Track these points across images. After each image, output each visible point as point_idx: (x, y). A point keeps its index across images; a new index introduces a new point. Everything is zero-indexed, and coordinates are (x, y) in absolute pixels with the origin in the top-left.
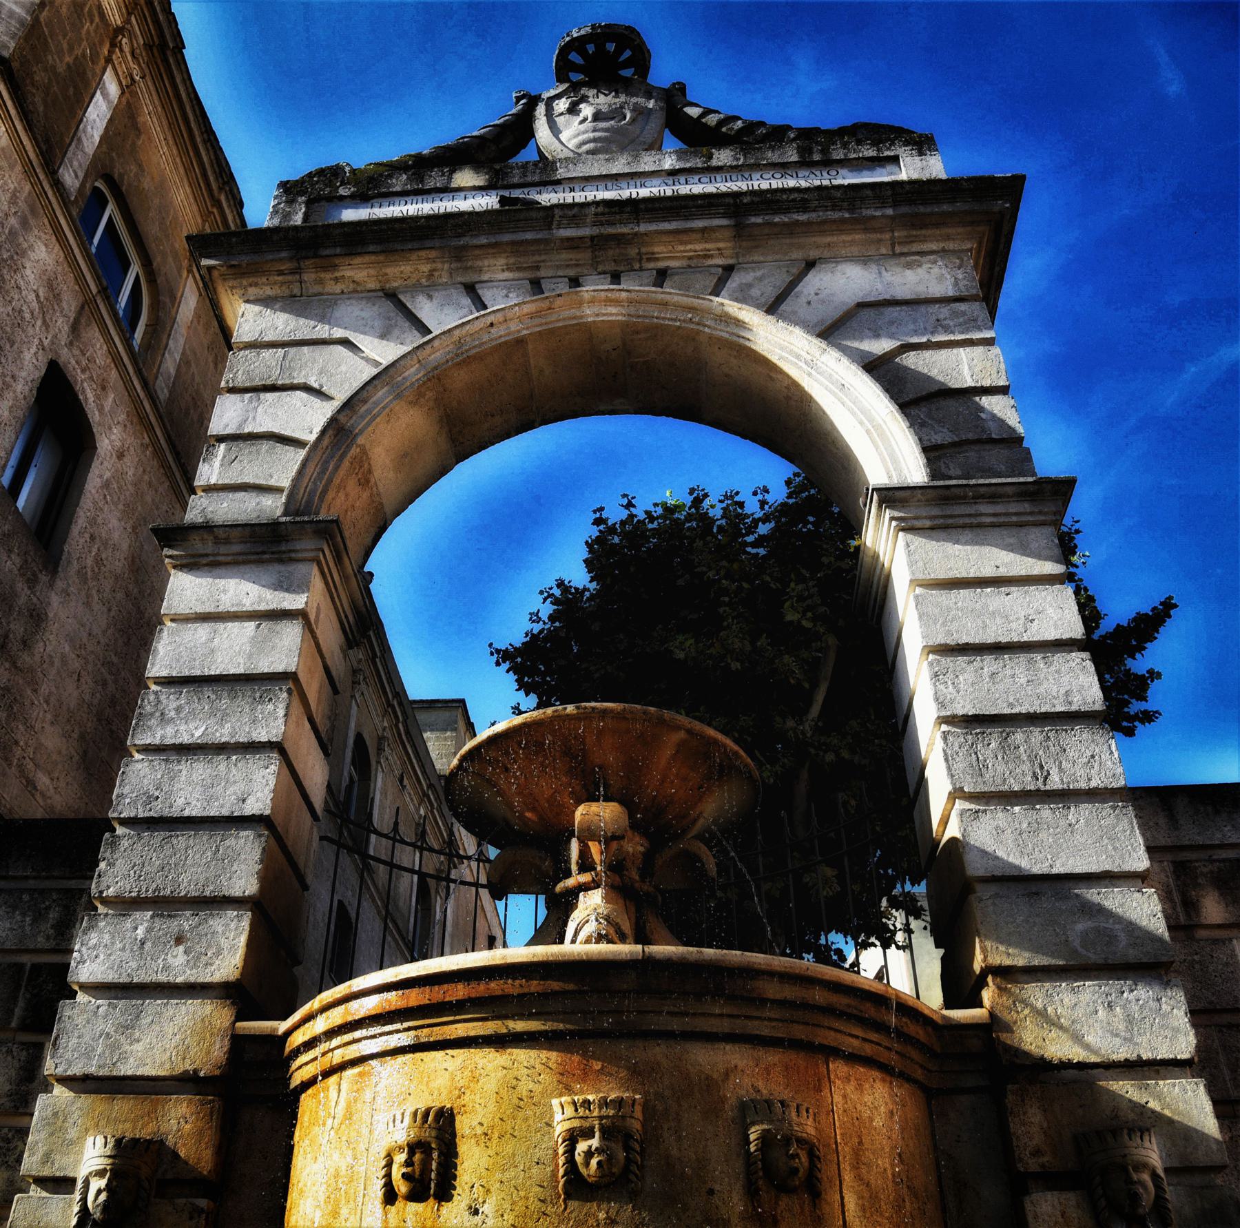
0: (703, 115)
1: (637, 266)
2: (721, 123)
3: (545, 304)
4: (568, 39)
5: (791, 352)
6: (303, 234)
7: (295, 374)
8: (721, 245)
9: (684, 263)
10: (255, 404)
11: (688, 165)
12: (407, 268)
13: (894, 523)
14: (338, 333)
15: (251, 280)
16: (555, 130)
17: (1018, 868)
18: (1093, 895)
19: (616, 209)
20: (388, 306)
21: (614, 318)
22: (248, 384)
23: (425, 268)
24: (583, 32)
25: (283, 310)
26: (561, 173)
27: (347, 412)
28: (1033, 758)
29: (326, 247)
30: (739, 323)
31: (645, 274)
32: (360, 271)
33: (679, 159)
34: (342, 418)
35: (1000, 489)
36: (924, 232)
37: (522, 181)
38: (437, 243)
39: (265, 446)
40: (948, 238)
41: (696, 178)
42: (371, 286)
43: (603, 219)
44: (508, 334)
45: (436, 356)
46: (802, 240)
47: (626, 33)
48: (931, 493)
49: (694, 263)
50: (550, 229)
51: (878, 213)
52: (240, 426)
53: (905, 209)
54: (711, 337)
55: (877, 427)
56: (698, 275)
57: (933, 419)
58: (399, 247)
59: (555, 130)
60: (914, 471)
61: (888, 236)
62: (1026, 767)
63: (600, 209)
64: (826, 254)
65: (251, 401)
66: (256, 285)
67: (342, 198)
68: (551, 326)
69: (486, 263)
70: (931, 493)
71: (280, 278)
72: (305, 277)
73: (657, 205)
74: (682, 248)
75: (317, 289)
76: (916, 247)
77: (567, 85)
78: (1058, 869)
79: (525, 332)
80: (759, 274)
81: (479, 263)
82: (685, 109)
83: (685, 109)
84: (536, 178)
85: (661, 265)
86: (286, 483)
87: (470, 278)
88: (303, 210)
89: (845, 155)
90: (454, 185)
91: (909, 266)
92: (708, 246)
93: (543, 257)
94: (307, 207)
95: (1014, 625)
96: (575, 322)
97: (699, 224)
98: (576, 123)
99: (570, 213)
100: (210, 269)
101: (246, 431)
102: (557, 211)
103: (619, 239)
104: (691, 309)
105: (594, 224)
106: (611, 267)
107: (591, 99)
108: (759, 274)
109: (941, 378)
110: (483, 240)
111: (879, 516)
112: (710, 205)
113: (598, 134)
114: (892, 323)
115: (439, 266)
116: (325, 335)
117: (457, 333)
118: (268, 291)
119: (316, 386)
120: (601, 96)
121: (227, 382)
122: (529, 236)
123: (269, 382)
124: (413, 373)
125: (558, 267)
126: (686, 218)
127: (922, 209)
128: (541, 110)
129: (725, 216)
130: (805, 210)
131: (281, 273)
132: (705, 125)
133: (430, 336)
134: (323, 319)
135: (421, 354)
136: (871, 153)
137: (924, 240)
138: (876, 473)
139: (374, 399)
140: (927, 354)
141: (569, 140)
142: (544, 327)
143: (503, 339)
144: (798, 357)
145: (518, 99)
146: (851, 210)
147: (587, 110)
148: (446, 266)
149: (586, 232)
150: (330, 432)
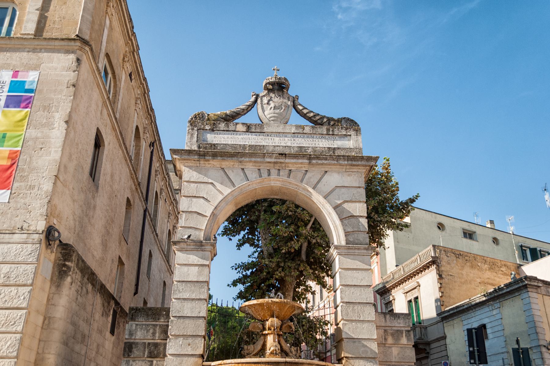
0: (303, 109)
1: (284, 168)
2: (307, 113)
3: (262, 180)
4: (268, 81)
5: (319, 201)
6: (201, 153)
7: (200, 193)
8: (305, 166)
9: (296, 169)
10: (191, 202)
11: (298, 132)
12: (227, 163)
13: (337, 253)
14: (210, 181)
15: (187, 161)
16: (263, 111)
17: (352, 336)
18: (365, 343)
19: (281, 155)
20: (222, 173)
21: (278, 185)
22: (188, 195)
23: (232, 164)
24: (272, 80)
25: (195, 171)
26: (265, 130)
27: (216, 210)
28: (358, 312)
29: (207, 157)
30: (308, 191)
31: (286, 171)
32: (216, 163)
33: (296, 129)
34: (214, 212)
35: (360, 248)
36: (354, 167)
37: (255, 131)
38: (236, 158)
39: (195, 215)
40: (359, 169)
41: (300, 135)
42: (218, 166)
43: (276, 157)
44: (253, 188)
45: (236, 194)
46: (324, 166)
47: (284, 81)
48: (346, 247)
49: (298, 169)
50: (264, 158)
51: (343, 163)
52: (188, 208)
53: (350, 162)
54: (301, 193)
55: (336, 226)
56: (299, 172)
57: (349, 224)
58: (226, 158)
59: (263, 111)
60: (343, 243)
61: (345, 167)
62: (356, 314)
63: (277, 155)
64: (330, 170)
65: (190, 201)
66: (188, 163)
67: (206, 130)
68: (263, 186)
69: (247, 164)
70: (346, 247)
71: (194, 162)
72: (201, 162)
73: (291, 155)
74: (295, 165)
75: (204, 165)
76: (351, 170)
77: (267, 91)
78: (360, 337)
79: (257, 187)
80: (313, 174)
81: (245, 164)
82: (298, 106)
83: (298, 106)
84: (259, 131)
85: (290, 169)
86: (204, 228)
87: (243, 167)
88: (197, 133)
89: (338, 133)
90: (237, 130)
91: (349, 175)
92: (302, 165)
93: (262, 164)
94: (197, 132)
95: (358, 281)
96: (269, 185)
97: (300, 161)
98: (269, 109)
99: (269, 155)
100: (176, 158)
101: (190, 210)
102: (266, 154)
103: (281, 163)
104: (297, 185)
105: (275, 158)
106: (278, 168)
107: (273, 99)
108: (313, 174)
109: (352, 212)
110: (247, 159)
111: (334, 250)
112: (304, 157)
113: (275, 115)
114: (343, 194)
115: (235, 163)
116: (207, 181)
117: (241, 187)
118: (191, 164)
119: (206, 198)
120: (276, 98)
121: (183, 194)
122: (259, 160)
123: (194, 195)
124: (230, 198)
125: (265, 167)
126: (298, 159)
127: (354, 163)
128: (259, 101)
129: (307, 159)
130: (326, 160)
131: (194, 161)
132: (303, 112)
133: (235, 188)
134: (205, 175)
135: (233, 193)
136: (344, 133)
137: (354, 169)
138: (336, 243)
139: (222, 205)
140: (350, 204)
141: (267, 115)
142: (262, 186)
143: (251, 189)
144: (320, 203)
145: (253, 95)
146: (337, 161)
147: (272, 105)
148: (237, 164)
149: (273, 160)
150: (212, 216)
